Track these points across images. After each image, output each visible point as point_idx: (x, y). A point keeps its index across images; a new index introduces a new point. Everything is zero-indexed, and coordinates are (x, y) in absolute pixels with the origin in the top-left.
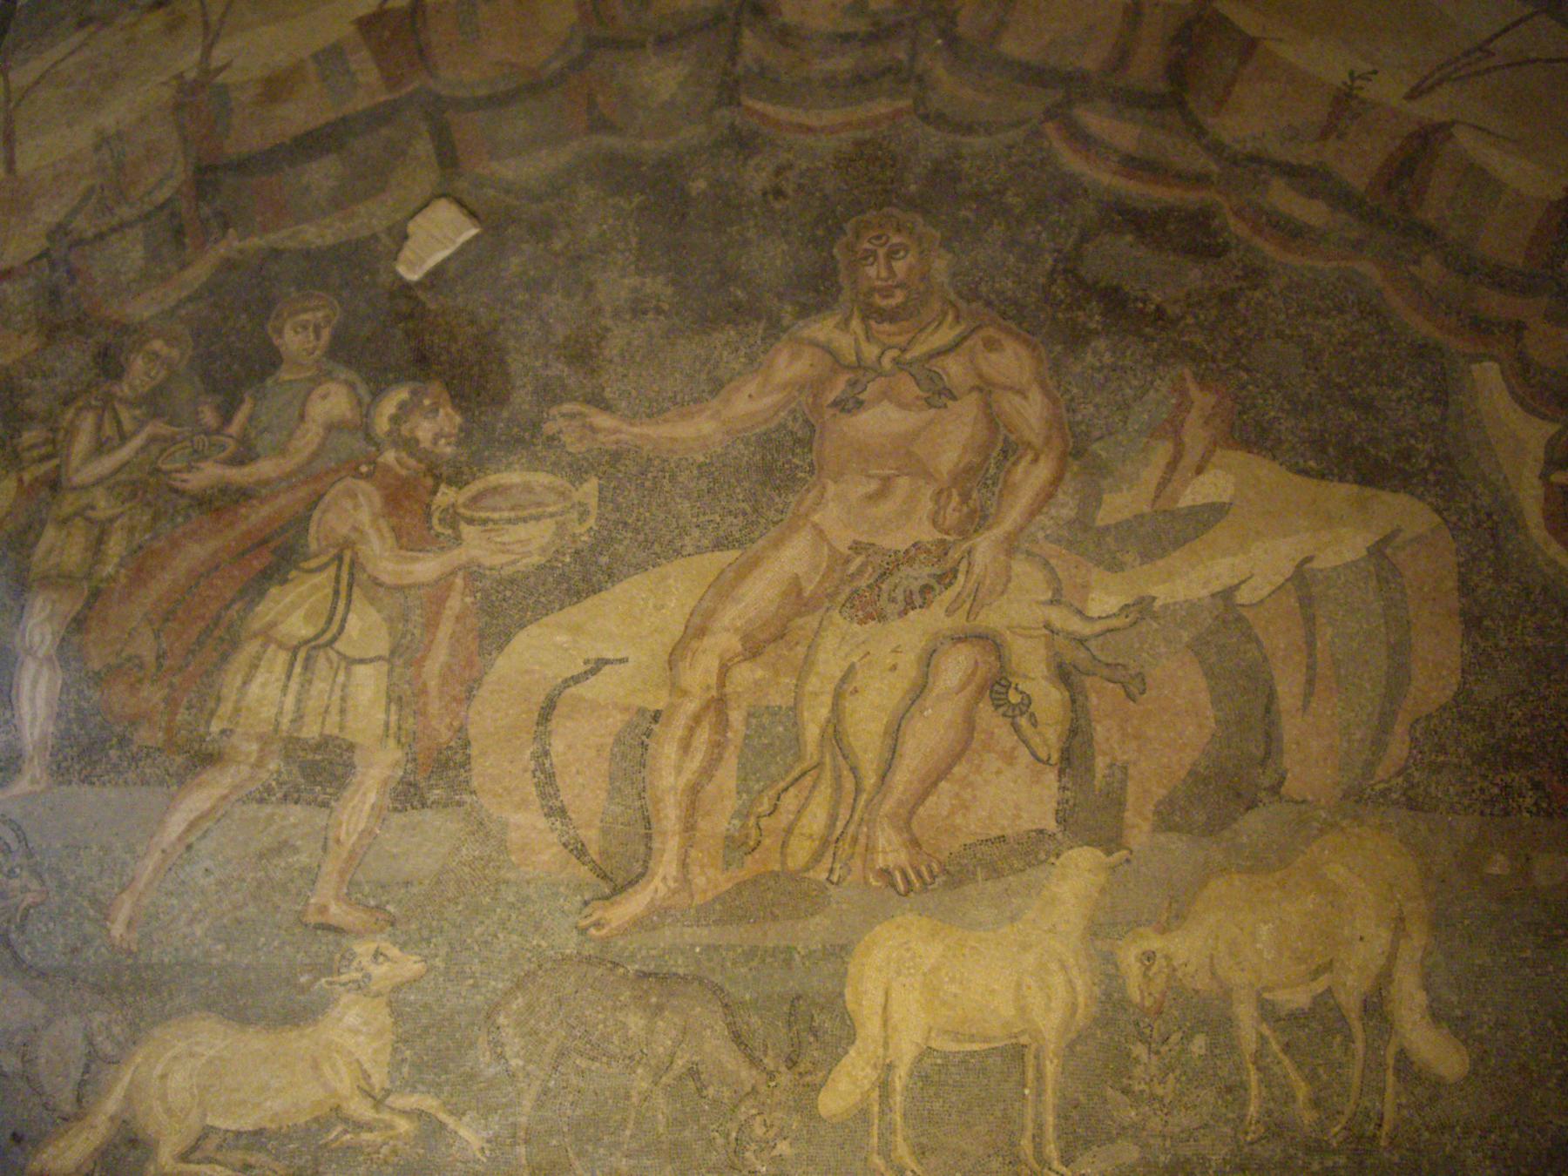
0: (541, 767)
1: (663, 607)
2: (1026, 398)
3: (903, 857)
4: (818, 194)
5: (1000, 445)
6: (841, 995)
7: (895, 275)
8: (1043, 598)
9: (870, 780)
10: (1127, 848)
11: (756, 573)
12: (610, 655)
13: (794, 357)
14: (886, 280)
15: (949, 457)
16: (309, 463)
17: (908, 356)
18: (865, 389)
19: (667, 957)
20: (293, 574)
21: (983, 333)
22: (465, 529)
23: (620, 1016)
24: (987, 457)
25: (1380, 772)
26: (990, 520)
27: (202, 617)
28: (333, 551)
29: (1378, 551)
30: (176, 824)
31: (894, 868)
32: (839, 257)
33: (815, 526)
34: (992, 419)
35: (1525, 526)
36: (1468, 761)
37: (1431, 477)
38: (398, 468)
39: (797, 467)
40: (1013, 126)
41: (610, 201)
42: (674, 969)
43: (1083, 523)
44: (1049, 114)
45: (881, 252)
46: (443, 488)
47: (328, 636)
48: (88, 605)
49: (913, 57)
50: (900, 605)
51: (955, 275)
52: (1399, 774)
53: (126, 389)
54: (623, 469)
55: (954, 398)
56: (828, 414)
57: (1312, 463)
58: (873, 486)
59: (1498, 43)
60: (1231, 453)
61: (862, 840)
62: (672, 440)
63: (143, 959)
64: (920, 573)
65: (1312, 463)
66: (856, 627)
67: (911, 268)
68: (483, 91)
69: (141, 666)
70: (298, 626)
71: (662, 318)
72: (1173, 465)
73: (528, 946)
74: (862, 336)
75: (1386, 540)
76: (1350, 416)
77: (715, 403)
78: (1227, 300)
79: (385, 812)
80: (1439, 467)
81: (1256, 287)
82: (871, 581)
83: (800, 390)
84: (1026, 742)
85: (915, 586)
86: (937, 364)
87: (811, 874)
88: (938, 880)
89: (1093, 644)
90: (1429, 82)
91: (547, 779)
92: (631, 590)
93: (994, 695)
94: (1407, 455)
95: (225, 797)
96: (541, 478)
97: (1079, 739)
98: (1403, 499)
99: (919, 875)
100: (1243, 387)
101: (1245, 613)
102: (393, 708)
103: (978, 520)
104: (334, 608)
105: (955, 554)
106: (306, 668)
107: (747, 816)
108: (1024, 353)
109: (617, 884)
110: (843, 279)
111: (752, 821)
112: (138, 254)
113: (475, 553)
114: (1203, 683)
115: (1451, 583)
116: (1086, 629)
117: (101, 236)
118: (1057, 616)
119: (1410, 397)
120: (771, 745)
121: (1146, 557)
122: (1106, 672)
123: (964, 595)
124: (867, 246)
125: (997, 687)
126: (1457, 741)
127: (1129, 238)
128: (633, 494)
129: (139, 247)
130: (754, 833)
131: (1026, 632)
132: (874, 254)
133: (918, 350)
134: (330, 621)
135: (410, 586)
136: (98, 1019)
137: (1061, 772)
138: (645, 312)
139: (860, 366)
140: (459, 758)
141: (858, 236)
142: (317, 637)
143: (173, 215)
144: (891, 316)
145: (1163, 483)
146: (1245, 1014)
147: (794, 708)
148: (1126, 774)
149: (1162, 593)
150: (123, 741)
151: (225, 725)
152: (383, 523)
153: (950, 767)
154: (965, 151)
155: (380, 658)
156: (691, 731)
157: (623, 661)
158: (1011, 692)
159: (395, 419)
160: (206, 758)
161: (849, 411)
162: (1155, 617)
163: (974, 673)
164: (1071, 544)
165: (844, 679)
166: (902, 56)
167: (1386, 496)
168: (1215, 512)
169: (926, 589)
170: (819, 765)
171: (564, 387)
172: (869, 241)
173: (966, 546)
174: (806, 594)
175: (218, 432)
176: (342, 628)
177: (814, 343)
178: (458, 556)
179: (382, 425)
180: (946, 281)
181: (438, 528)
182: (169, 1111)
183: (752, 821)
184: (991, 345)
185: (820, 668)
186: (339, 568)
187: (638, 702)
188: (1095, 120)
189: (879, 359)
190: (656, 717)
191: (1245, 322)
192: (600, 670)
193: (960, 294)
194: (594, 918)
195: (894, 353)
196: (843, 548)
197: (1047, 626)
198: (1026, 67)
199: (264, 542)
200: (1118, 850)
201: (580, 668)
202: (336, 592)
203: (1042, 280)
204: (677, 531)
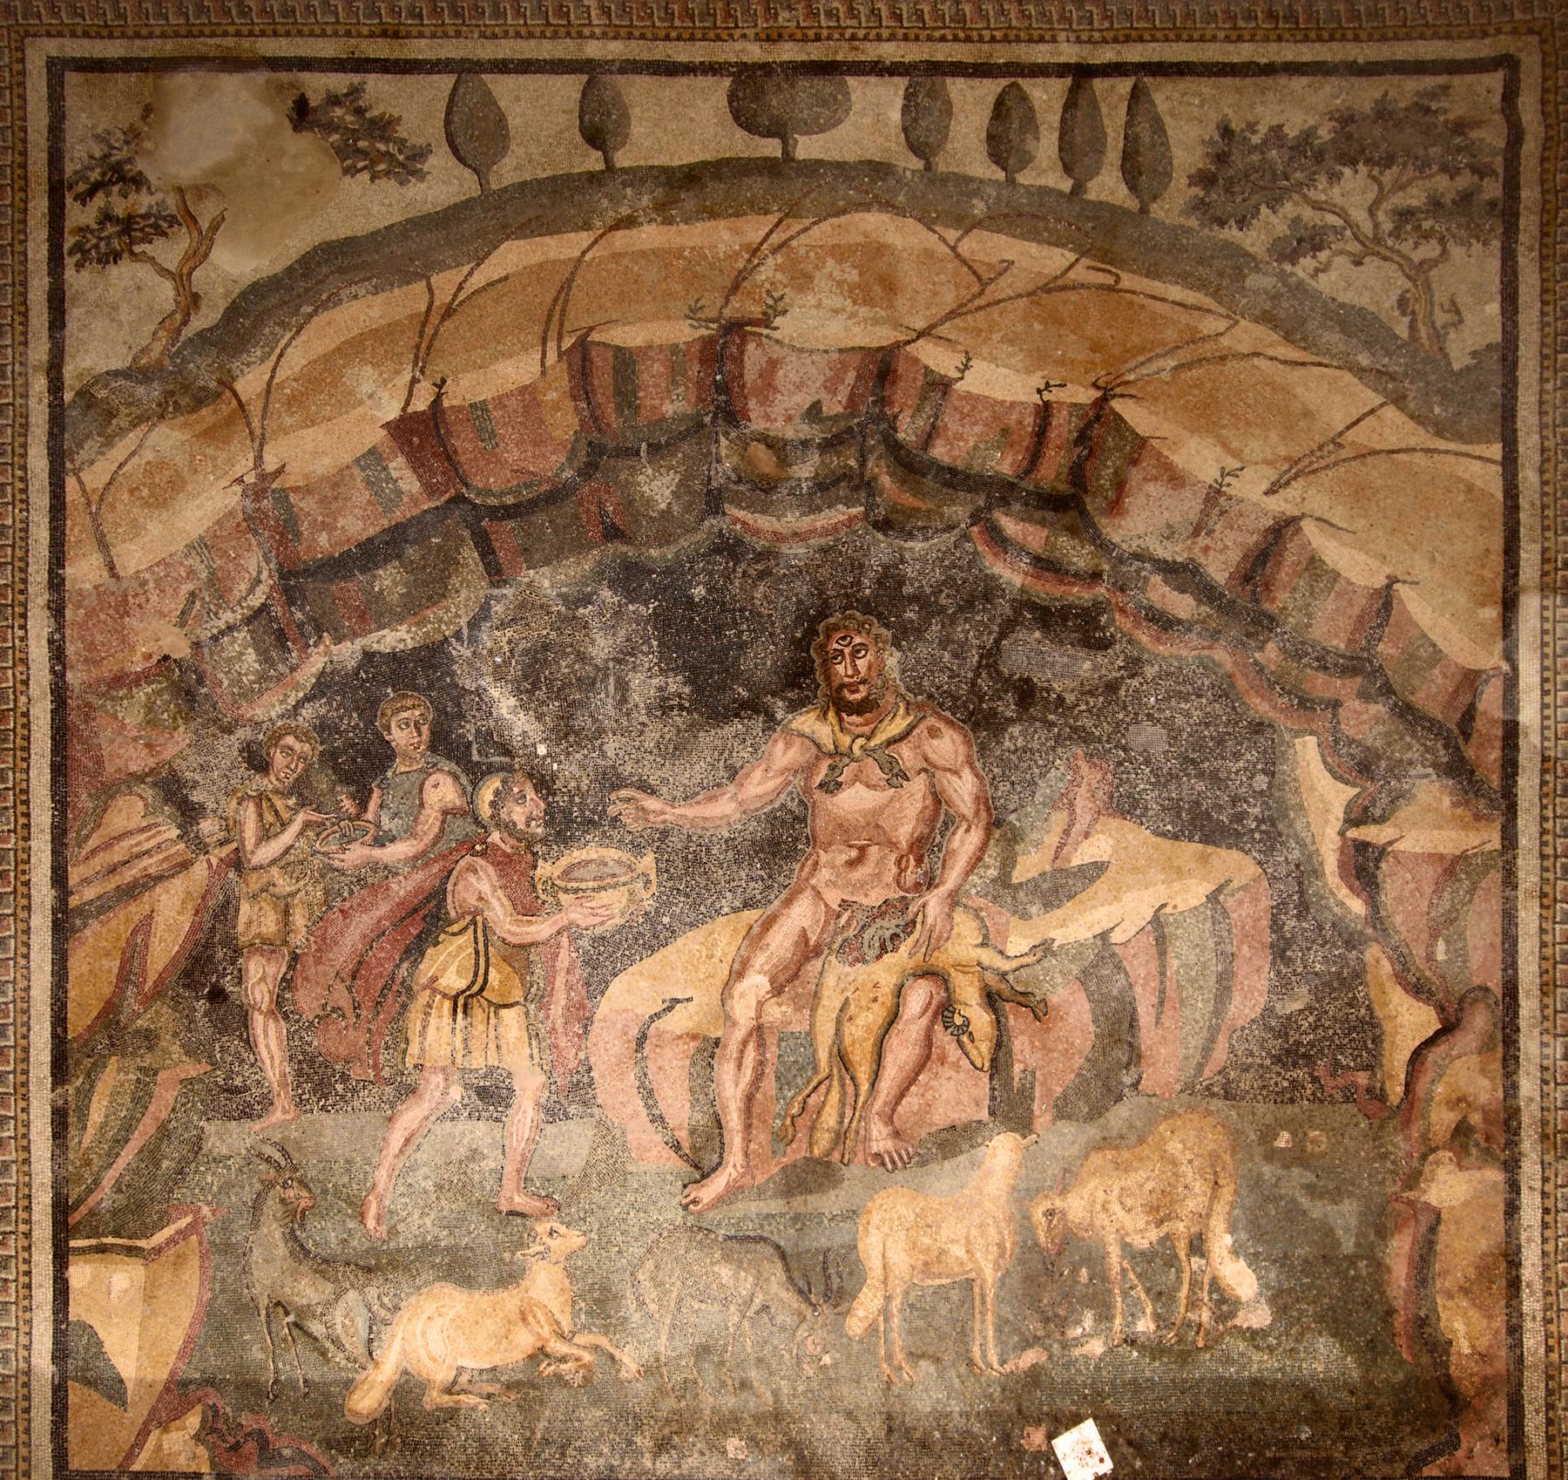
0: (642, 1086)
3: (889, 1144)
5: (942, 818)
11: (775, 927)
12: (680, 997)
15: (905, 832)
16: (434, 844)
17: (872, 744)
20: (442, 937)
22: (562, 896)
23: (716, 1269)
24: (932, 830)
25: (1207, 1072)
27: (381, 976)
28: (468, 918)
29: (1213, 898)
30: (396, 1139)
33: (814, 888)
34: (938, 799)
35: (1323, 874)
36: (1268, 1062)
37: (1257, 836)
38: (503, 845)
40: (944, 531)
41: (631, 608)
43: (1003, 880)
44: (976, 518)
45: (847, 651)
46: (540, 862)
47: (476, 988)
48: (291, 967)
49: (863, 464)
51: (904, 671)
52: (1219, 1073)
53: (273, 778)
56: (818, 795)
57: (1169, 827)
58: (854, 853)
59: (1350, 435)
60: (1111, 820)
61: (862, 1132)
62: (705, 819)
63: (392, 1245)
64: (890, 925)
65: (1169, 827)
66: (847, 969)
67: (869, 668)
68: (510, 500)
69: (344, 1017)
70: (454, 980)
72: (1067, 832)
74: (837, 728)
75: (1219, 890)
76: (1200, 786)
77: (731, 788)
78: (1112, 687)
79: (542, 1126)
80: (1263, 827)
81: (1132, 676)
84: (966, 1054)
85: (887, 934)
90: (1286, 477)
91: (648, 1094)
92: (689, 943)
94: (1240, 817)
95: (427, 1118)
96: (612, 854)
98: (1236, 855)
100: (1120, 764)
101: (1117, 949)
102: (534, 1043)
103: (930, 882)
104: (477, 965)
105: (913, 909)
106: (465, 1012)
108: (958, 738)
109: (702, 1171)
110: (819, 677)
111: (788, 1122)
112: (251, 656)
113: (573, 916)
114: (1087, 1006)
115: (1265, 923)
117: (215, 638)
118: (986, 956)
119: (1246, 769)
120: (796, 1062)
121: (1048, 906)
122: (1021, 999)
124: (836, 646)
126: (1263, 1048)
127: (1037, 634)
129: (250, 650)
130: (790, 1130)
134: (476, 974)
135: (531, 945)
136: (372, 1292)
137: (991, 1078)
140: (586, 1080)
141: (828, 637)
142: (469, 988)
143: (272, 620)
144: (860, 708)
145: (1061, 846)
146: (1114, 1252)
147: (810, 1033)
149: (1060, 936)
150: (345, 1078)
151: (416, 1061)
152: (500, 893)
153: (917, 1074)
154: (907, 556)
155: (517, 1003)
157: (689, 1000)
159: (493, 804)
160: (409, 1091)
162: (1054, 955)
164: (995, 899)
166: (852, 463)
167: (1223, 852)
168: (1099, 868)
169: (895, 937)
174: (812, 943)
175: (358, 817)
176: (486, 981)
178: (561, 919)
179: (485, 811)
180: (896, 675)
181: (543, 897)
182: (433, 1359)
184: (933, 733)
185: (825, 1002)
186: (475, 931)
188: (1010, 526)
190: (717, 1043)
191: (1125, 708)
193: (908, 689)
195: (861, 741)
196: (835, 907)
198: (953, 471)
199: (415, 910)
201: (659, 1007)
202: (477, 952)
203: (970, 675)
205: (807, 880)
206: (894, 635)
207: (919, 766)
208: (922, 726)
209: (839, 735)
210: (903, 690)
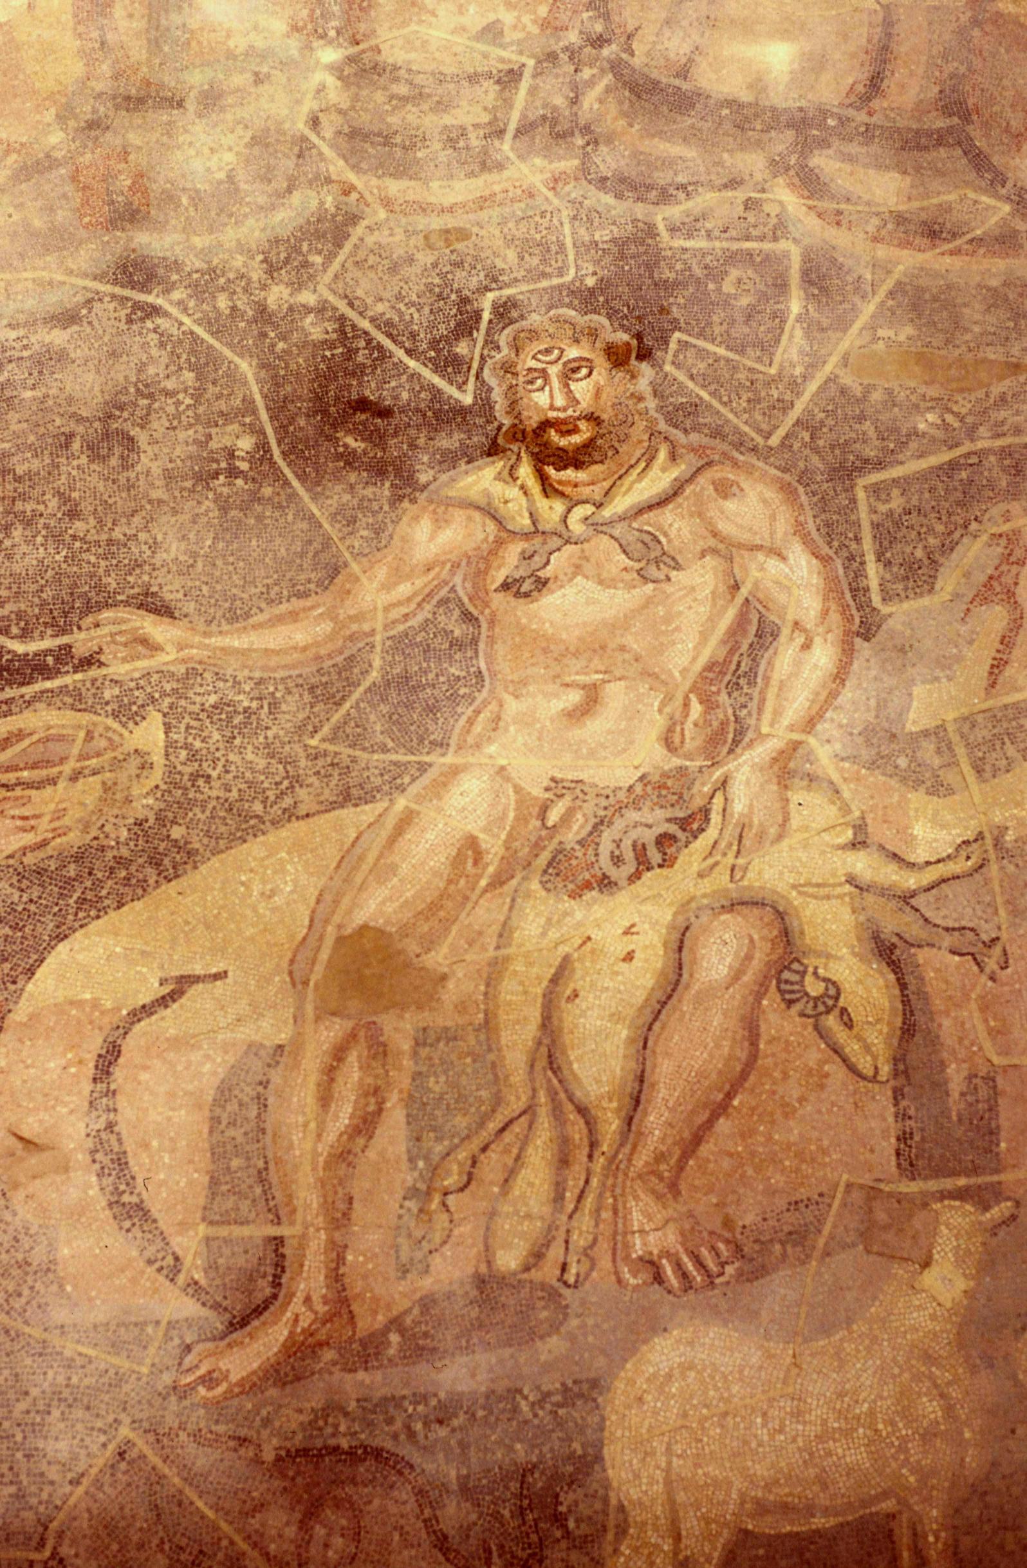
1: (273, 893)
2: (784, 559)
5: (753, 629)
6: (599, 1458)
7: (578, 402)
8: (841, 840)
9: (611, 1126)
10: (1008, 1199)
12: (198, 970)
13: (439, 523)
14: (565, 409)
17: (607, 513)
18: (548, 562)
19: (321, 1423)
21: (715, 473)
26: (750, 735)
31: (660, 1257)
39: (458, 678)
42: (332, 1442)
45: (554, 371)
50: (630, 868)
54: (198, 699)
55: (677, 567)
56: (499, 601)
58: (574, 697)
67: (598, 394)
71: (239, 482)
73: (99, 1424)
77: (327, 598)
82: (584, 833)
83: (456, 566)
87: (535, 1275)
88: (730, 1270)
89: (919, 901)
93: (783, 986)
97: (918, 1038)
99: (699, 1263)
107: (429, 1193)
116: (912, 881)
118: (861, 864)
123: (723, 845)
124: (533, 364)
125: (786, 975)
128: (216, 736)
131: (822, 892)
133: (621, 504)
138: (216, 475)
139: (536, 531)
144: (575, 459)
148: (995, 1087)
156: (330, 1073)
158: (809, 979)
161: (527, 595)
163: (749, 957)
165: (555, 980)
169: (663, 840)
170: (529, 1110)
171: (99, 588)
172: (534, 357)
173: (718, 774)
183: (437, 1199)
184: (724, 490)
187: (246, 1033)
189: (564, 520)
192: (182, 993)
194: (202, 1371)
196: (537, 792)
197: (851, 880)
200: (998, 1203)
204: (286, 783)
205: (478, 746)
207: (701, 544)
208: (703, 480)
210: (662, 426)
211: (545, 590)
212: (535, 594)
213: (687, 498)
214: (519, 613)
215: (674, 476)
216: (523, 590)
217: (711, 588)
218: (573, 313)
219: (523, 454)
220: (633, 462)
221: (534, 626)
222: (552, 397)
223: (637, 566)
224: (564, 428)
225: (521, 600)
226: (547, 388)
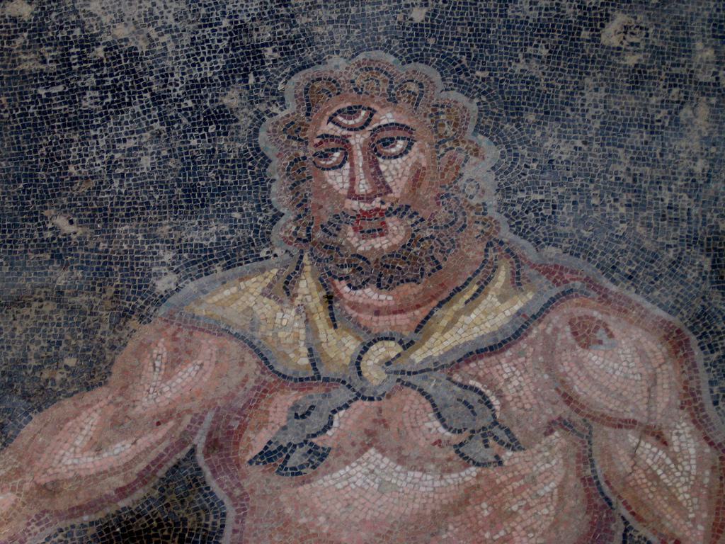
4: (225, 23)
7: (389, 190)
14: (369, 199)
17: (418, 356)
18: (329, 426)
32: (270, 150)
45: (358, 140)
55: (514, 445)
56: (256, 477)
67: (417, 178)
74: (321, 320)
86: (472, 374)
124: (328, 128)
132: (344, 145)
133: (438, 345)
139: (314, 377)
161: (296, 472)
172: (331, 120)
177: (220, 329)
180: (492, 201)
206: (484, 111)
209: (326, 334)
210: (506, 234)
211: (322, 466)
212: (308, 471)
213: (532, 343)
214: (283, 498)
215: (516, 308)
216: (290, 464)
217: (559, 479)
218: (392, 59)
219: (306, 260)
220: (460, 283)
221: (303, 520)
222: (353, 180)
223: (456, 439)
224: (367, 227)
225: (286, 480)
226: (347, 165)
